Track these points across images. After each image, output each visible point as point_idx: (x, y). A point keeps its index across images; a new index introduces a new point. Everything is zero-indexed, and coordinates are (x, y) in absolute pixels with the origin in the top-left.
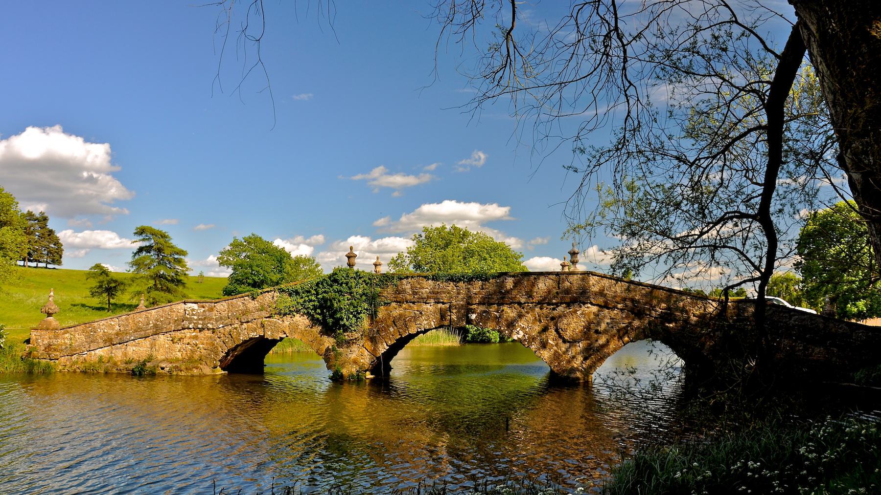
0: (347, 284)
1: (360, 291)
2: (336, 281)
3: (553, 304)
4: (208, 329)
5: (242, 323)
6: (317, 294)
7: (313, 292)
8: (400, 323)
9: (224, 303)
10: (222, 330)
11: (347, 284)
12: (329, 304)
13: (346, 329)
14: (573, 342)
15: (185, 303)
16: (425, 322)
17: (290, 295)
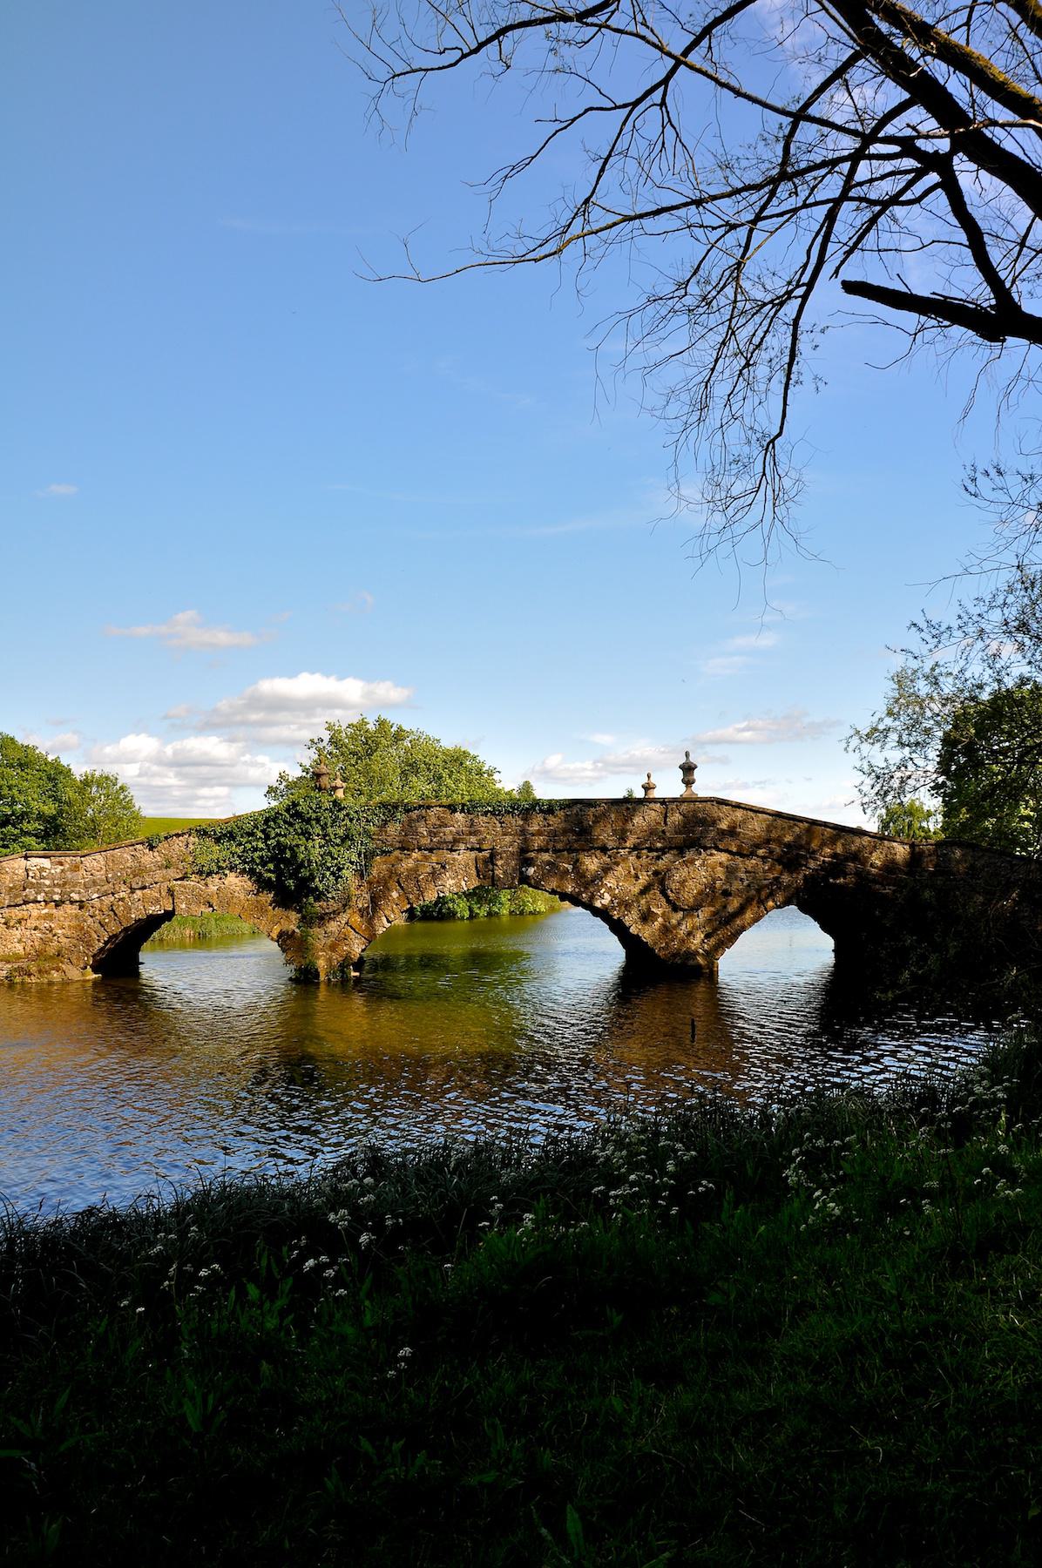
0: (318, 820)
1: (341, 832)
2: (298, 815)
3: (657, 850)
4: (72, 903)
5: (133, 891)
6: (267, 837)
7: (260, 834)
9: (98, 856)
10: (96, 903)
14: (692, 910)
15: (26, 857)
16: (451, 882)
17: (218, 840)
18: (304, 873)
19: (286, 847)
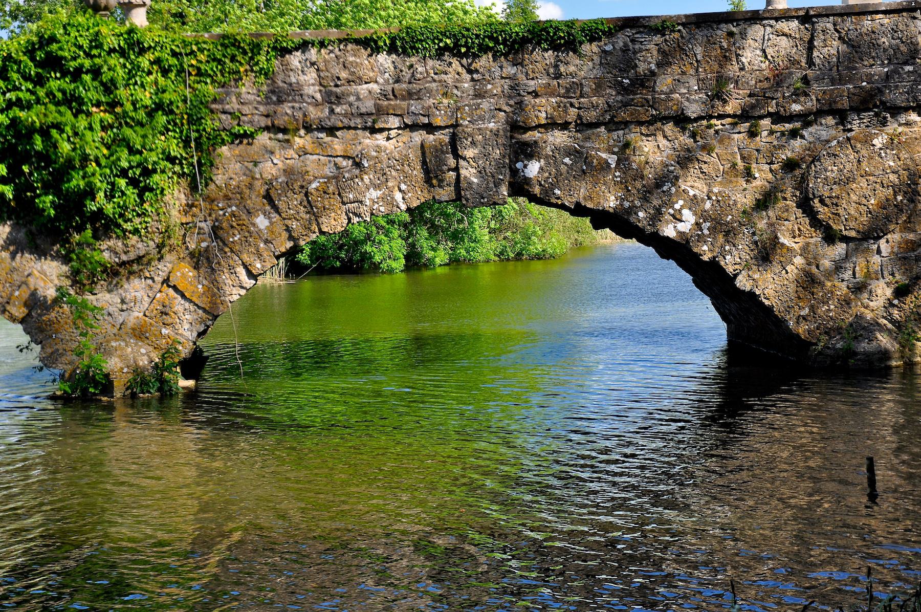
0: (96, 72)
1: (146, 97)
2: (54, 63)
3: (790, 118)
8: (292, 203)
11: (96, 72)
12: (38, 143)
13: (104, 226)
14: (872, 233)
16: (374, 194)
18: (77, 182)
19: (32, 130)
